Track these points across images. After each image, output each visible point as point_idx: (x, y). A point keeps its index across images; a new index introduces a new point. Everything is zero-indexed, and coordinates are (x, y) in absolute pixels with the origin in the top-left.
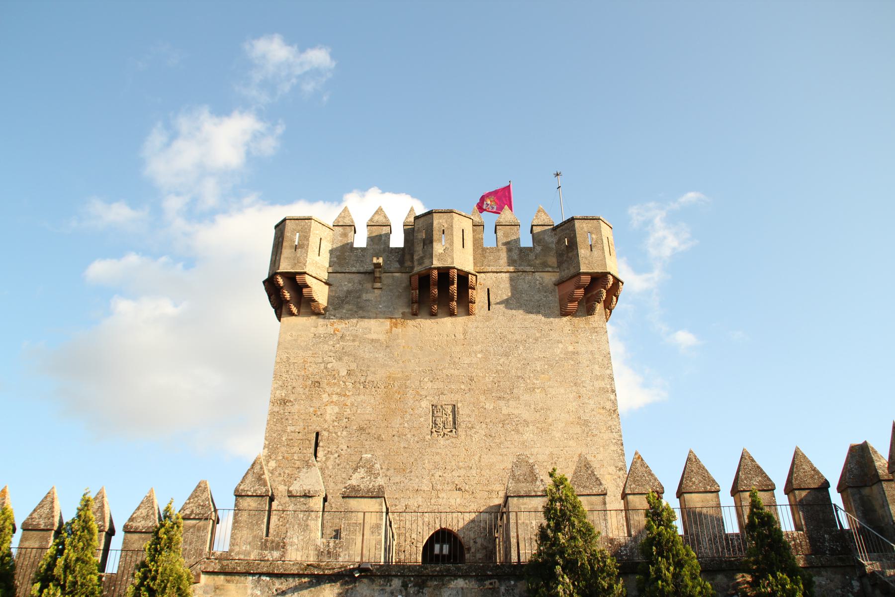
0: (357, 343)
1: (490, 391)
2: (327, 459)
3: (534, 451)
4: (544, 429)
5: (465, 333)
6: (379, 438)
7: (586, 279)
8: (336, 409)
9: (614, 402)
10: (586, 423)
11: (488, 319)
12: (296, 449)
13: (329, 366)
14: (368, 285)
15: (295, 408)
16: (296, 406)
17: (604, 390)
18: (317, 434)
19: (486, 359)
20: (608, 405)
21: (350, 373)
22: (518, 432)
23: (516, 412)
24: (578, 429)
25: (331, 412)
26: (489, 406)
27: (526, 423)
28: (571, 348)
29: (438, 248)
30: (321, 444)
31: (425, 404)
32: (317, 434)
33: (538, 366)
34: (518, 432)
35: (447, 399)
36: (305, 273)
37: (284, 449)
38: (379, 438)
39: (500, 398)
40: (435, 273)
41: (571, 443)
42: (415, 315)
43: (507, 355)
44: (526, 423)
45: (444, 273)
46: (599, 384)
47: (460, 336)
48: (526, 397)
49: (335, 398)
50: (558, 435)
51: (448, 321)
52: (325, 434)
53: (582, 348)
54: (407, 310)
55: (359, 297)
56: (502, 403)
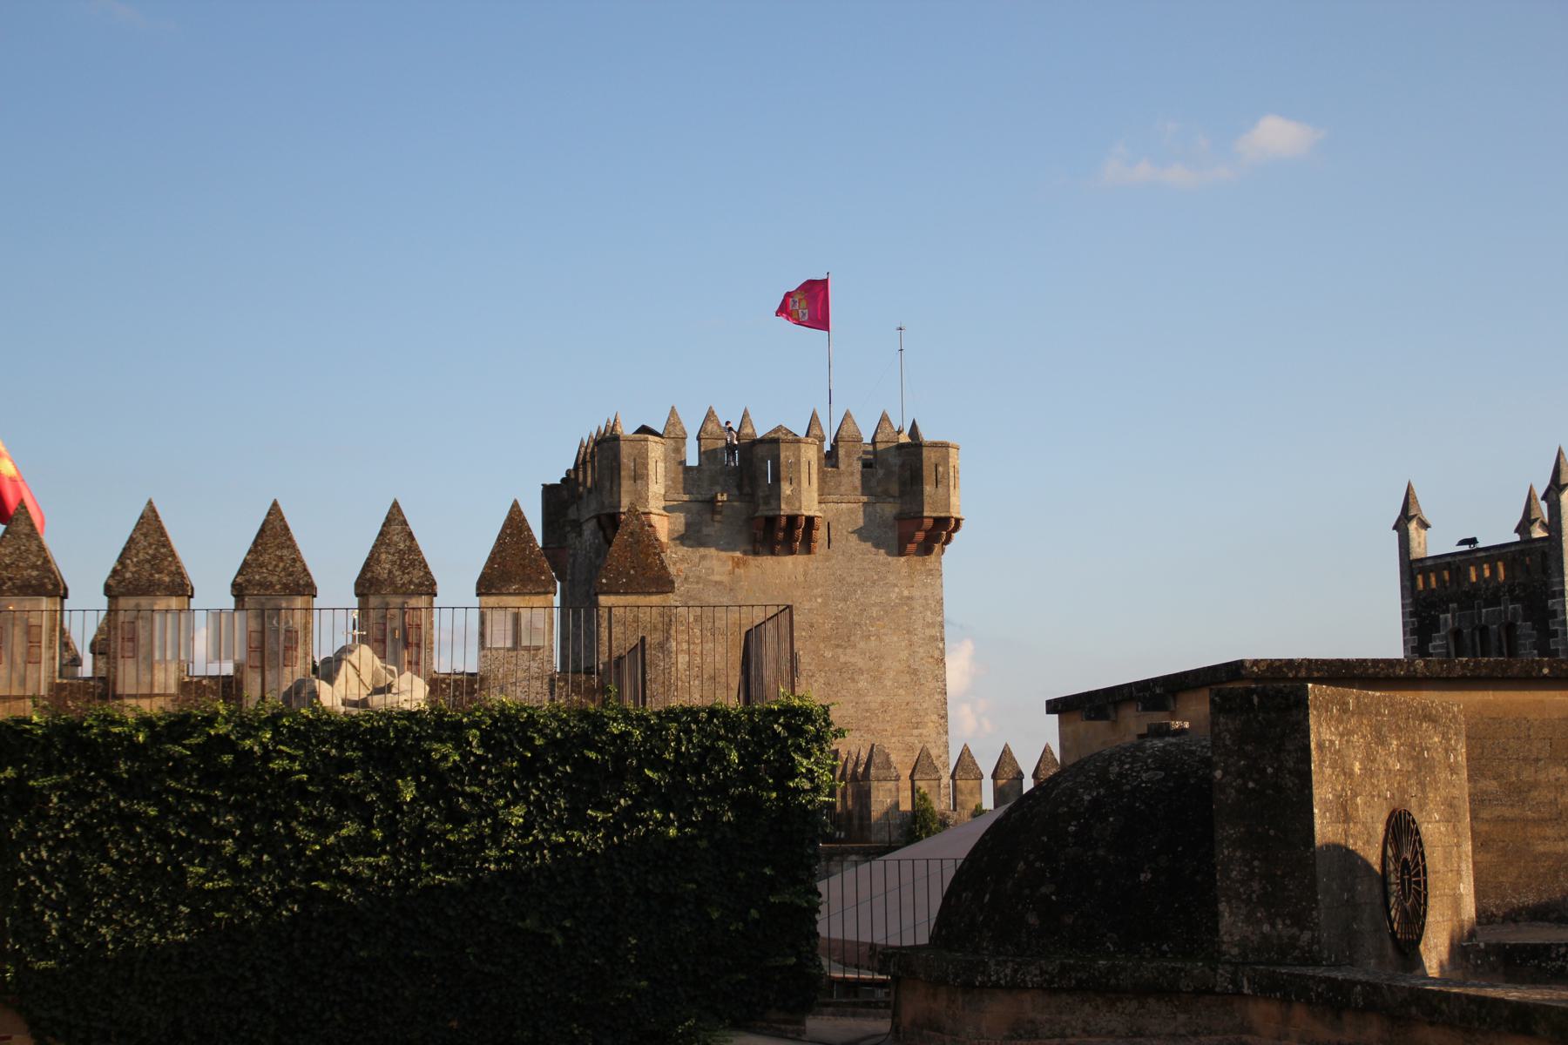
1: (828, 638)
3: (868, 699)
4: (877, 679)
5: (805, 574)
7: (928, 524)
9: (942, 652)
10: (915, 672)
11: (827, 559)
14: (708, 517)
17: (933, 639)
19: (825, 604)
20: (937, 654)
22: (853, 680)
23: (853, 660)
24: (907, 678)
26: (828, 654)
27: (861, 672)
28: (906, 593)
29: (786, 489)
33: (874, 612)
34: (853, 680)
39: (838, 646)
40: (784, 521)
41: (901, 692)
42: (756, 553)
43: (845, 600)
44: (861, 672)
45: (793, 520)
46: (929, 632)
47: (801, 578)
48: (862, 645)
50: (889, 683)
51: (789, 560)
53: (916, 593)
54: (750, 548)
55: (699, 531)
56: (840, 651)
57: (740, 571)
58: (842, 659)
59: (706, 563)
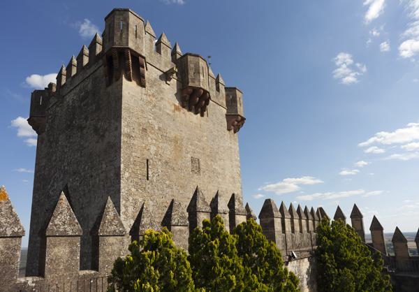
0: (161, 112)
2: (153, 176)
4: (224, 178)
6: (173, 169)
8: (155, 149)
12: (138, 167)
13: (150, 121)
15: (135, 142)
16: (136, 141)
18: (147, 160)
21: (159, 129)
25: (153, 149)
30: (150, 167)
31: (189, 156)
32: (147, 160)
35: (196, 156)
36: (144, 58)
37: (132, 166)
38: (173, 169)
49: (154, 141)
52: (151, 161)
57: (177, 112)
58: (214, 167)
59: (164, 102)
